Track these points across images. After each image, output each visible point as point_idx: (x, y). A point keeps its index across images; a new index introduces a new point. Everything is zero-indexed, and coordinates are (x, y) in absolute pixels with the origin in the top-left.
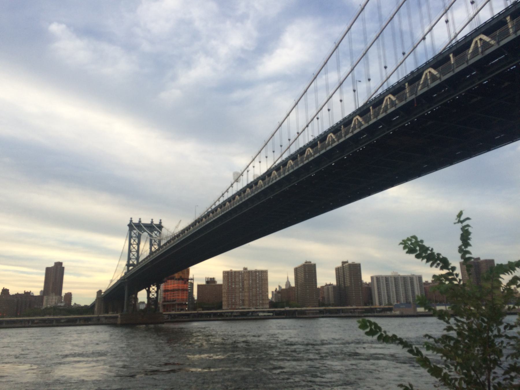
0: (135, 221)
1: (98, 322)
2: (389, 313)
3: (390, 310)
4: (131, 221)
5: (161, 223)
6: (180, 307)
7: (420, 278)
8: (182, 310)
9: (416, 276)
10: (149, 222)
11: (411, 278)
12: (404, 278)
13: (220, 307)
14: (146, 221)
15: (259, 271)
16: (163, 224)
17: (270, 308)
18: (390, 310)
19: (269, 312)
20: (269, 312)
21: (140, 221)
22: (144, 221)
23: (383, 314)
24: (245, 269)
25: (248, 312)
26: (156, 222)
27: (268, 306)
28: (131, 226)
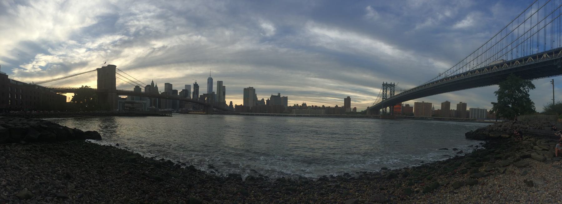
0: (385, 83)
1: (367, 117)
2: (474, 121)
3: (475, 120)
4: (383, 83)
5: (394, 84)
6: (398, 114)
7: (486, 110)
8: (399, 115)
9: (485, 109)
10: (390, 83)
11: (483, 110)
12: (481, 110)
13: (413, 115)
14: (389, 83)
15: (428, 103)
16: (395, 84)
17: (432, 116)
18: (475, 120)
19: (432, 118)
20: (432, 118)
21: (387, 83)
22: (388, 83)
23: (472, 121)
24: (423, 102)
25: (424, 118)
26: (393, 83)
27: (431, 116)
28: (384, 85)
